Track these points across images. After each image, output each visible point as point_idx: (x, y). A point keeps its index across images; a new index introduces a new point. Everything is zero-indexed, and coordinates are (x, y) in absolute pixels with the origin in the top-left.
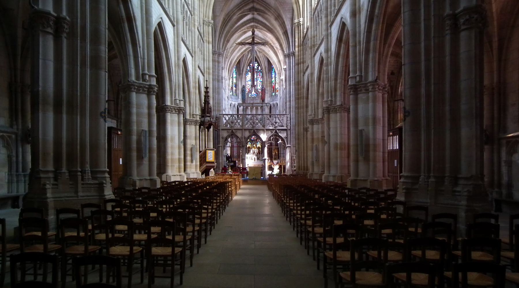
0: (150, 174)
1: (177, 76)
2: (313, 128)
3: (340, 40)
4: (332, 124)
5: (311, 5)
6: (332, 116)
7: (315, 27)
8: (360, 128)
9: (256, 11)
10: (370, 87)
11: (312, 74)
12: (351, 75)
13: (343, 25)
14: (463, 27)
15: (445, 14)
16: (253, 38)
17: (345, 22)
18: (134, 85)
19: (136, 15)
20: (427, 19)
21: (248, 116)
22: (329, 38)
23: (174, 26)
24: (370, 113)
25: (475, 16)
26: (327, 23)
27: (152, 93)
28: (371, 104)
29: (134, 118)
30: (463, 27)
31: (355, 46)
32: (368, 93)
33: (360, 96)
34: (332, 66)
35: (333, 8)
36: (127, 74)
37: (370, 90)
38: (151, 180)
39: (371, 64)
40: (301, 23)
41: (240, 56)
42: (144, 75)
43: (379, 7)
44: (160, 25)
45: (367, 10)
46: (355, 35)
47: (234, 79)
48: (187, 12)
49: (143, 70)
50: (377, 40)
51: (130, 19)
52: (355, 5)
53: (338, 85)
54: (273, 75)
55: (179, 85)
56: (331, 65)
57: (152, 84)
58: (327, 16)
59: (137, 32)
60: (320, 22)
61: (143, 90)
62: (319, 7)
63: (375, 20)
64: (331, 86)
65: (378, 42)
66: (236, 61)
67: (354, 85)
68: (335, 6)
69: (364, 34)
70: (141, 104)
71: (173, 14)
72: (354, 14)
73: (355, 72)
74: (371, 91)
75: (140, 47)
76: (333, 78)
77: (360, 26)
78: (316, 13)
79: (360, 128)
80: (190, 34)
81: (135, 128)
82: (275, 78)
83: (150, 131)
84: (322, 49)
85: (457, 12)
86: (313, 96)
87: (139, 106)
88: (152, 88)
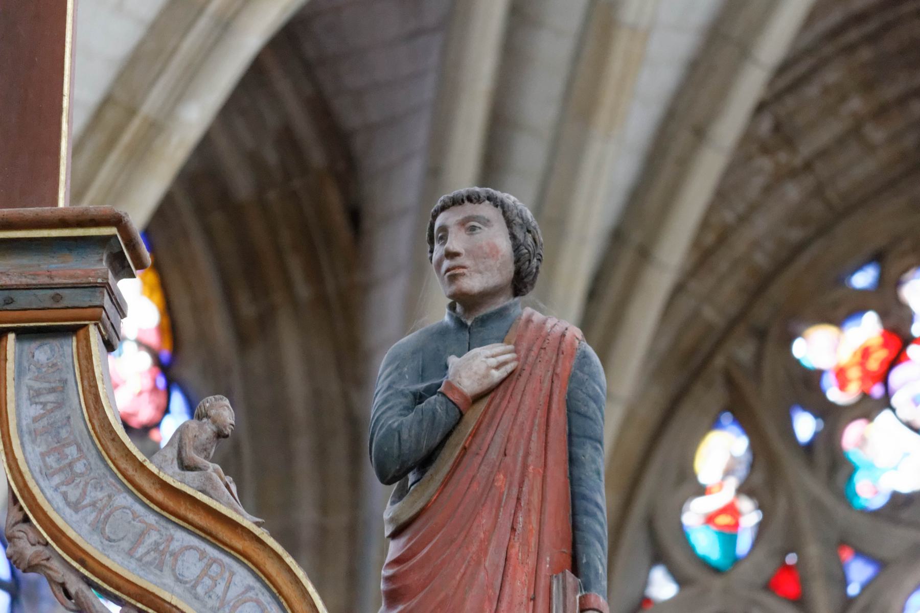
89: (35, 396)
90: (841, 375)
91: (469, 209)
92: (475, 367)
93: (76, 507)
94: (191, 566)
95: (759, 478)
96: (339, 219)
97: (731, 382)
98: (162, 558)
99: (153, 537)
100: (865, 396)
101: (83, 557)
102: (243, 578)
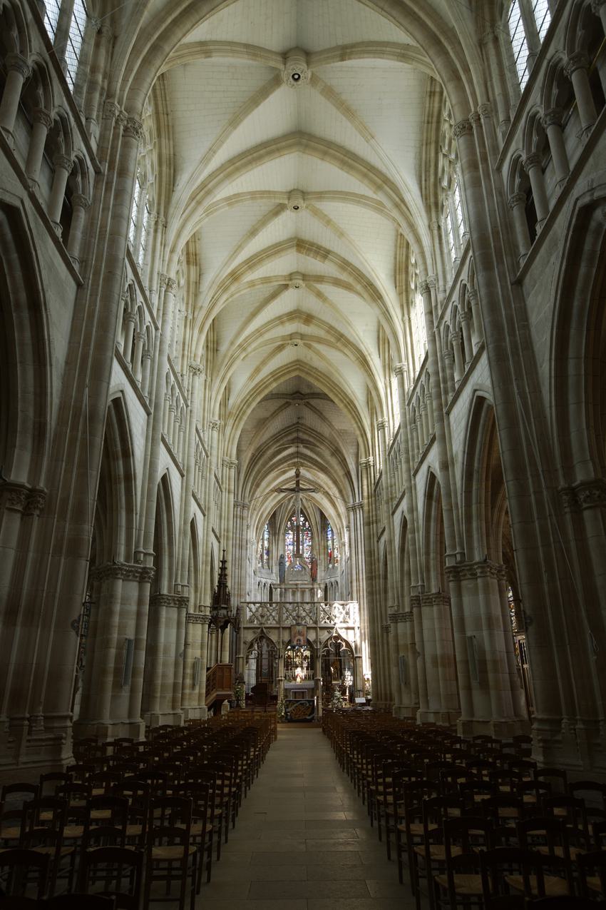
0: (130, 714)
1: (181, 547)
2: (396, 628)
3: (429, 496)
4: (426, 623)
5: (385, 442)
6: (425, 610)
7: (392, 472)
8: (469, 634)
9: (302, 443)
10: (478, 571)
11: (391, 541)
12: (448, 552)
13: (432, 478)
14: (585, 505)
15: (560, 488)
16: (298, 483)
17: (434, 472)
18: (121, 569)
19: (137, 471)
20: (538, 493)
21: (288, 605)
22: (413, 491)
23: (182, 476)
24: (482, 610)
25: (597, 493)
26: (409, 470)
27: (147, 579)
28: (481, 597)
29: (116, 619)
30: (585, 505)
31: (450, 510)
32: (477, 578)
33: (464, 583)
34: (421, 532)
35: (416, 451)
36: (112, 553)
37: (479, 575)
38: (130, 724)
39: (475, 536)
40: (371, 463)
42: (137, 553)
43: (479, 459)
44: (165, 479)
45: (463, 463)
46: (449, 495)
47: (266, 543)
48: (201, 453)
49: (137, 546)
50: (480, 503)
51: (129, 477)
52: (446, 454)
53: (432, 562)
54: (330, 536)
55: (183, 563)
56: (418, 532)
57: (148, 566)
58: (408, 461)
59: (136, 494)
60: (399, 466)
61: (134, 576)
62: (395, 445)
63: (475, 476)
64: (420, 564)
65: (483, 505)
66: (269, 513)
67: (453, 567)
68: (418, 449)
69: (462, 494)
70: (127, 594)
71: (183, 460)
72: (446, 466)
73: (454, 548)
74: (480, 577)
75: (136, 514)
76: (423, 551)
77: (455, 484)
78: (392, 453)
79: (469, 634)
80: (203, 482)
81: (115, 636)
82: (333, 540)
83: (137, 640)
84: (404, 505)
85: (573, 485)
86: (394, 576)
87: (125, 600)
88: (147, 573)
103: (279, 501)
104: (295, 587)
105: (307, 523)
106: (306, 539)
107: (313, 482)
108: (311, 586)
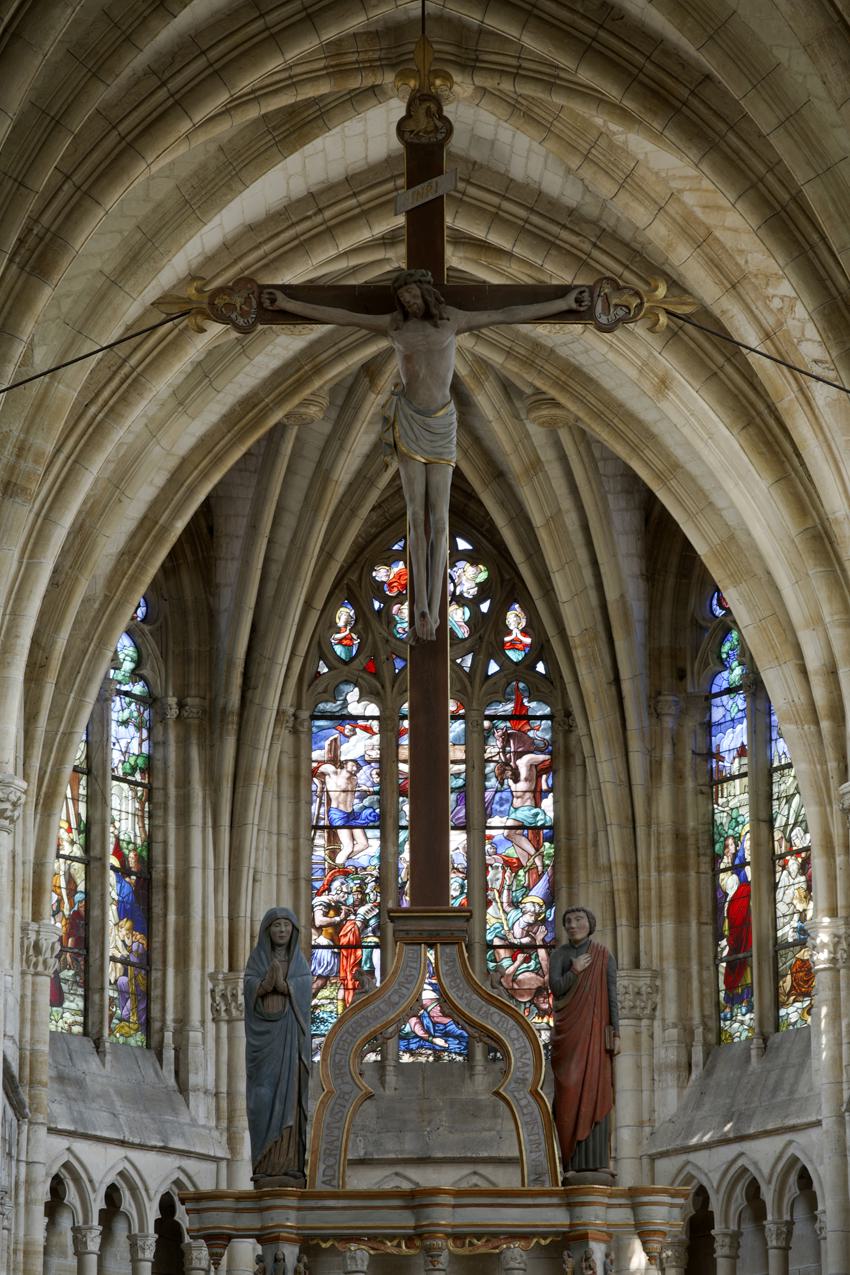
16: (425, 234)
41: (208, 448)
47: (122, 802)
54: (731, 739)
66: (149, 525)
82: (763, 777)
89: (446, 963)
90: (390, 584)
91: (578, 914)
92: (582, 962)
93: (461, 998)
94: (496, 1018)
95: (360, 626)
96: (205, 531)
97: (349, 589)
98: (487, 1015)
99: (484, 1009)
100: (400, 593)
101: (464, 1015)
102: (512, 1022)
103: (249, 409)
104: (405, 1220)
105: (515, 619)
106: (508, 770)
107: (573, 218)
108: (557, 1217)
